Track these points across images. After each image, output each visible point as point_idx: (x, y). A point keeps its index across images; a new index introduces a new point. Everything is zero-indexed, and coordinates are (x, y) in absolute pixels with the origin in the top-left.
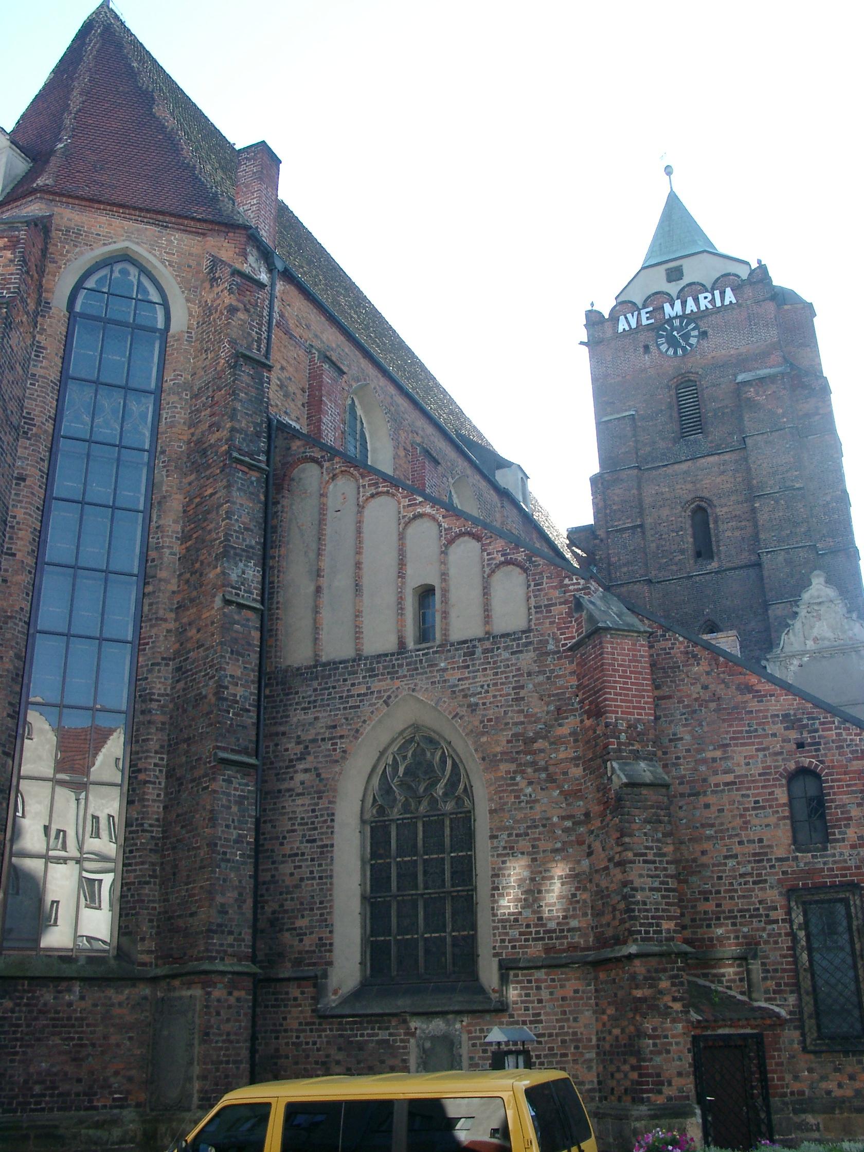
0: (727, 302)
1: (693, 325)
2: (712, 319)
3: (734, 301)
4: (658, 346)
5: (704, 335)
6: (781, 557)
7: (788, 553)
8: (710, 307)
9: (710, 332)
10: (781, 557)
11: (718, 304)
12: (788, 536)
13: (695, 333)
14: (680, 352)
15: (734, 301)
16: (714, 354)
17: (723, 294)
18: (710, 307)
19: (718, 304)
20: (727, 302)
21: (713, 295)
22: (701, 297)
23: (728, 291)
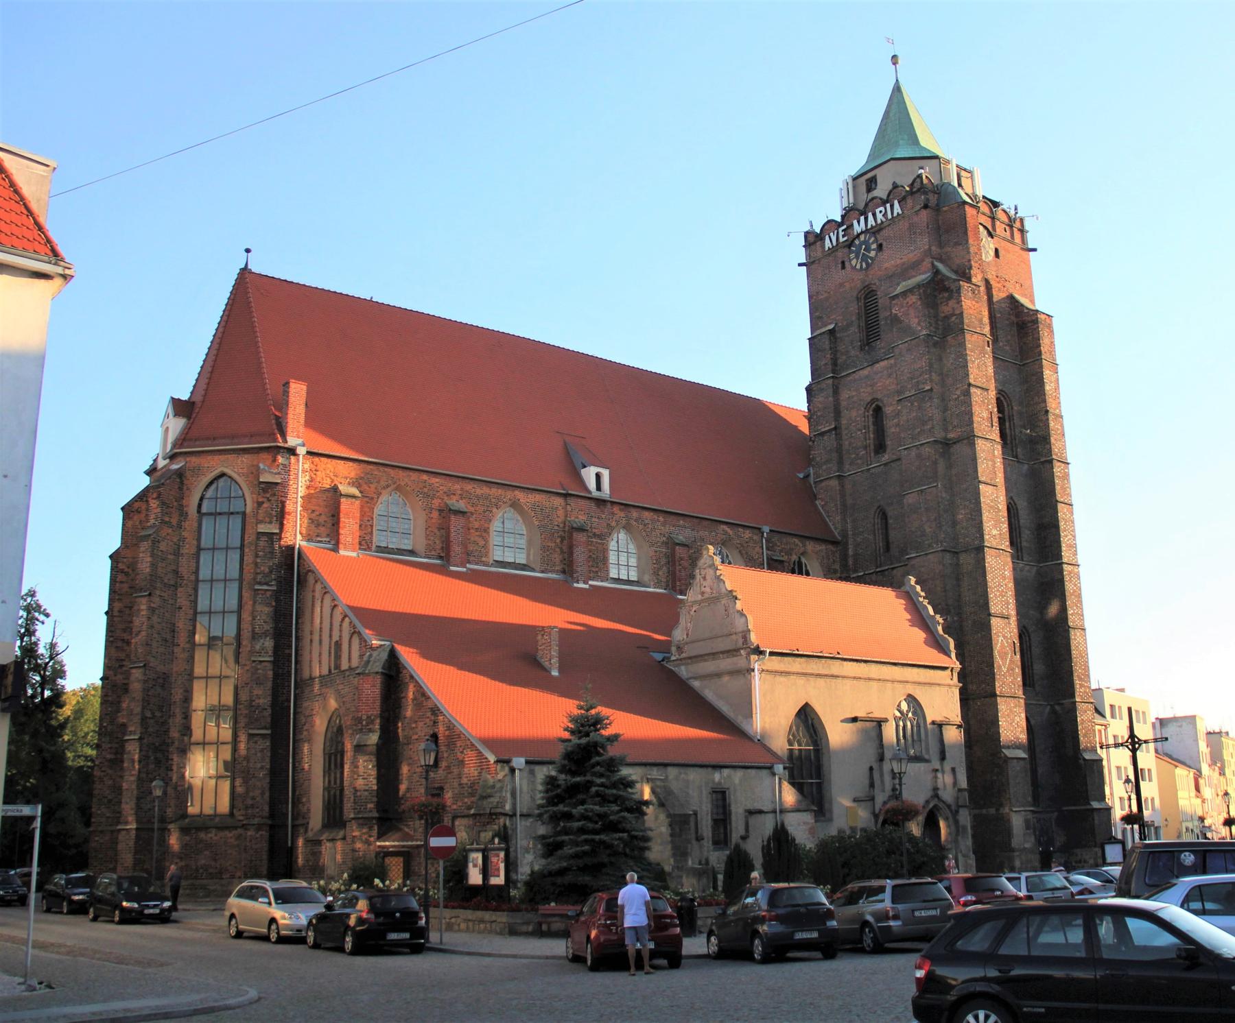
0: (895, 214)
1: (873, 239)
2: (884, 233)
3: (900, 212)
4: (850, 260)
5: (880, 247)
6: (913, 453)
7: (918, 448)
8: (884, 220)
9: (884, 244)
10: (913, 453)
11: (890, 216)
12: (919, 433)
13: (874, 246)
14: (864, 266)
15: (900, 212)
16: (886, 265)
17: (892, 206)
18: (884, 220)
19: (890, 216)
20: (879, 222)
21: (886, 209)
22: (877, 211)
23: (896, 202)
